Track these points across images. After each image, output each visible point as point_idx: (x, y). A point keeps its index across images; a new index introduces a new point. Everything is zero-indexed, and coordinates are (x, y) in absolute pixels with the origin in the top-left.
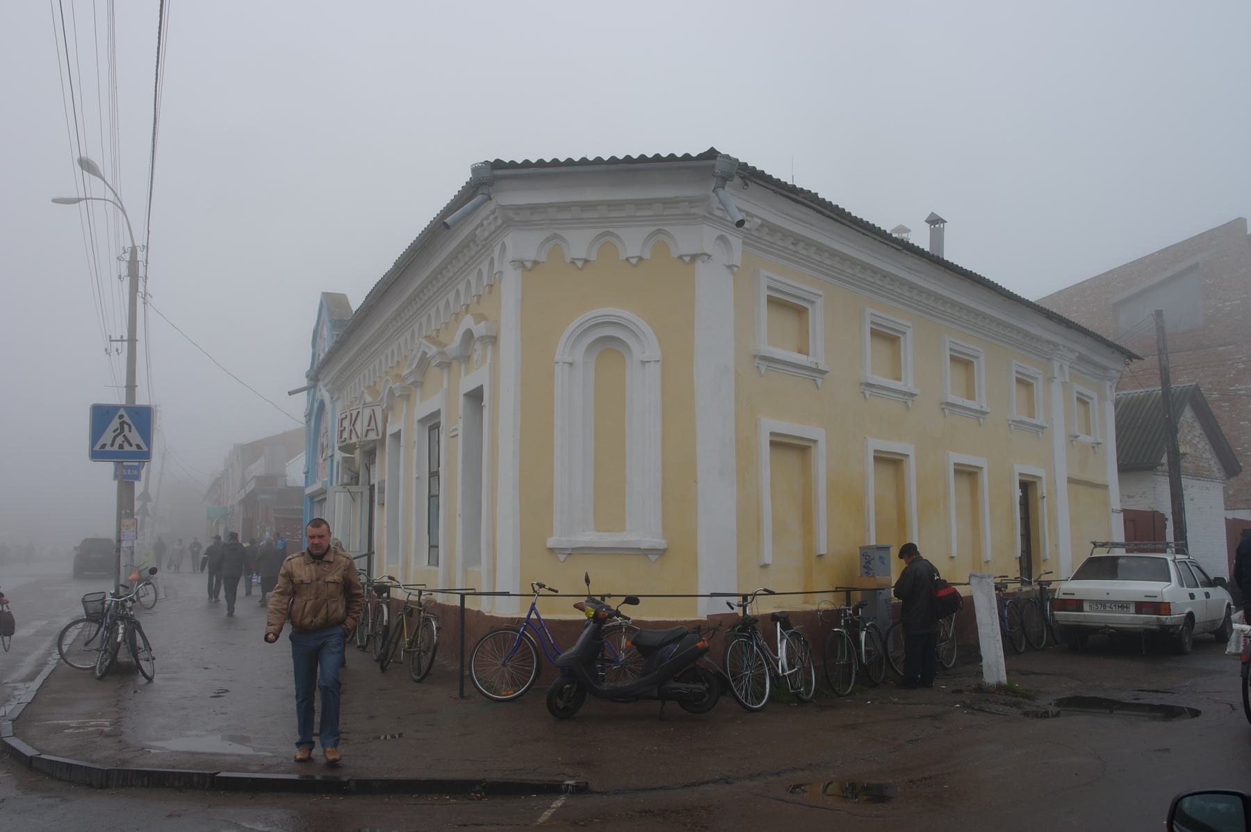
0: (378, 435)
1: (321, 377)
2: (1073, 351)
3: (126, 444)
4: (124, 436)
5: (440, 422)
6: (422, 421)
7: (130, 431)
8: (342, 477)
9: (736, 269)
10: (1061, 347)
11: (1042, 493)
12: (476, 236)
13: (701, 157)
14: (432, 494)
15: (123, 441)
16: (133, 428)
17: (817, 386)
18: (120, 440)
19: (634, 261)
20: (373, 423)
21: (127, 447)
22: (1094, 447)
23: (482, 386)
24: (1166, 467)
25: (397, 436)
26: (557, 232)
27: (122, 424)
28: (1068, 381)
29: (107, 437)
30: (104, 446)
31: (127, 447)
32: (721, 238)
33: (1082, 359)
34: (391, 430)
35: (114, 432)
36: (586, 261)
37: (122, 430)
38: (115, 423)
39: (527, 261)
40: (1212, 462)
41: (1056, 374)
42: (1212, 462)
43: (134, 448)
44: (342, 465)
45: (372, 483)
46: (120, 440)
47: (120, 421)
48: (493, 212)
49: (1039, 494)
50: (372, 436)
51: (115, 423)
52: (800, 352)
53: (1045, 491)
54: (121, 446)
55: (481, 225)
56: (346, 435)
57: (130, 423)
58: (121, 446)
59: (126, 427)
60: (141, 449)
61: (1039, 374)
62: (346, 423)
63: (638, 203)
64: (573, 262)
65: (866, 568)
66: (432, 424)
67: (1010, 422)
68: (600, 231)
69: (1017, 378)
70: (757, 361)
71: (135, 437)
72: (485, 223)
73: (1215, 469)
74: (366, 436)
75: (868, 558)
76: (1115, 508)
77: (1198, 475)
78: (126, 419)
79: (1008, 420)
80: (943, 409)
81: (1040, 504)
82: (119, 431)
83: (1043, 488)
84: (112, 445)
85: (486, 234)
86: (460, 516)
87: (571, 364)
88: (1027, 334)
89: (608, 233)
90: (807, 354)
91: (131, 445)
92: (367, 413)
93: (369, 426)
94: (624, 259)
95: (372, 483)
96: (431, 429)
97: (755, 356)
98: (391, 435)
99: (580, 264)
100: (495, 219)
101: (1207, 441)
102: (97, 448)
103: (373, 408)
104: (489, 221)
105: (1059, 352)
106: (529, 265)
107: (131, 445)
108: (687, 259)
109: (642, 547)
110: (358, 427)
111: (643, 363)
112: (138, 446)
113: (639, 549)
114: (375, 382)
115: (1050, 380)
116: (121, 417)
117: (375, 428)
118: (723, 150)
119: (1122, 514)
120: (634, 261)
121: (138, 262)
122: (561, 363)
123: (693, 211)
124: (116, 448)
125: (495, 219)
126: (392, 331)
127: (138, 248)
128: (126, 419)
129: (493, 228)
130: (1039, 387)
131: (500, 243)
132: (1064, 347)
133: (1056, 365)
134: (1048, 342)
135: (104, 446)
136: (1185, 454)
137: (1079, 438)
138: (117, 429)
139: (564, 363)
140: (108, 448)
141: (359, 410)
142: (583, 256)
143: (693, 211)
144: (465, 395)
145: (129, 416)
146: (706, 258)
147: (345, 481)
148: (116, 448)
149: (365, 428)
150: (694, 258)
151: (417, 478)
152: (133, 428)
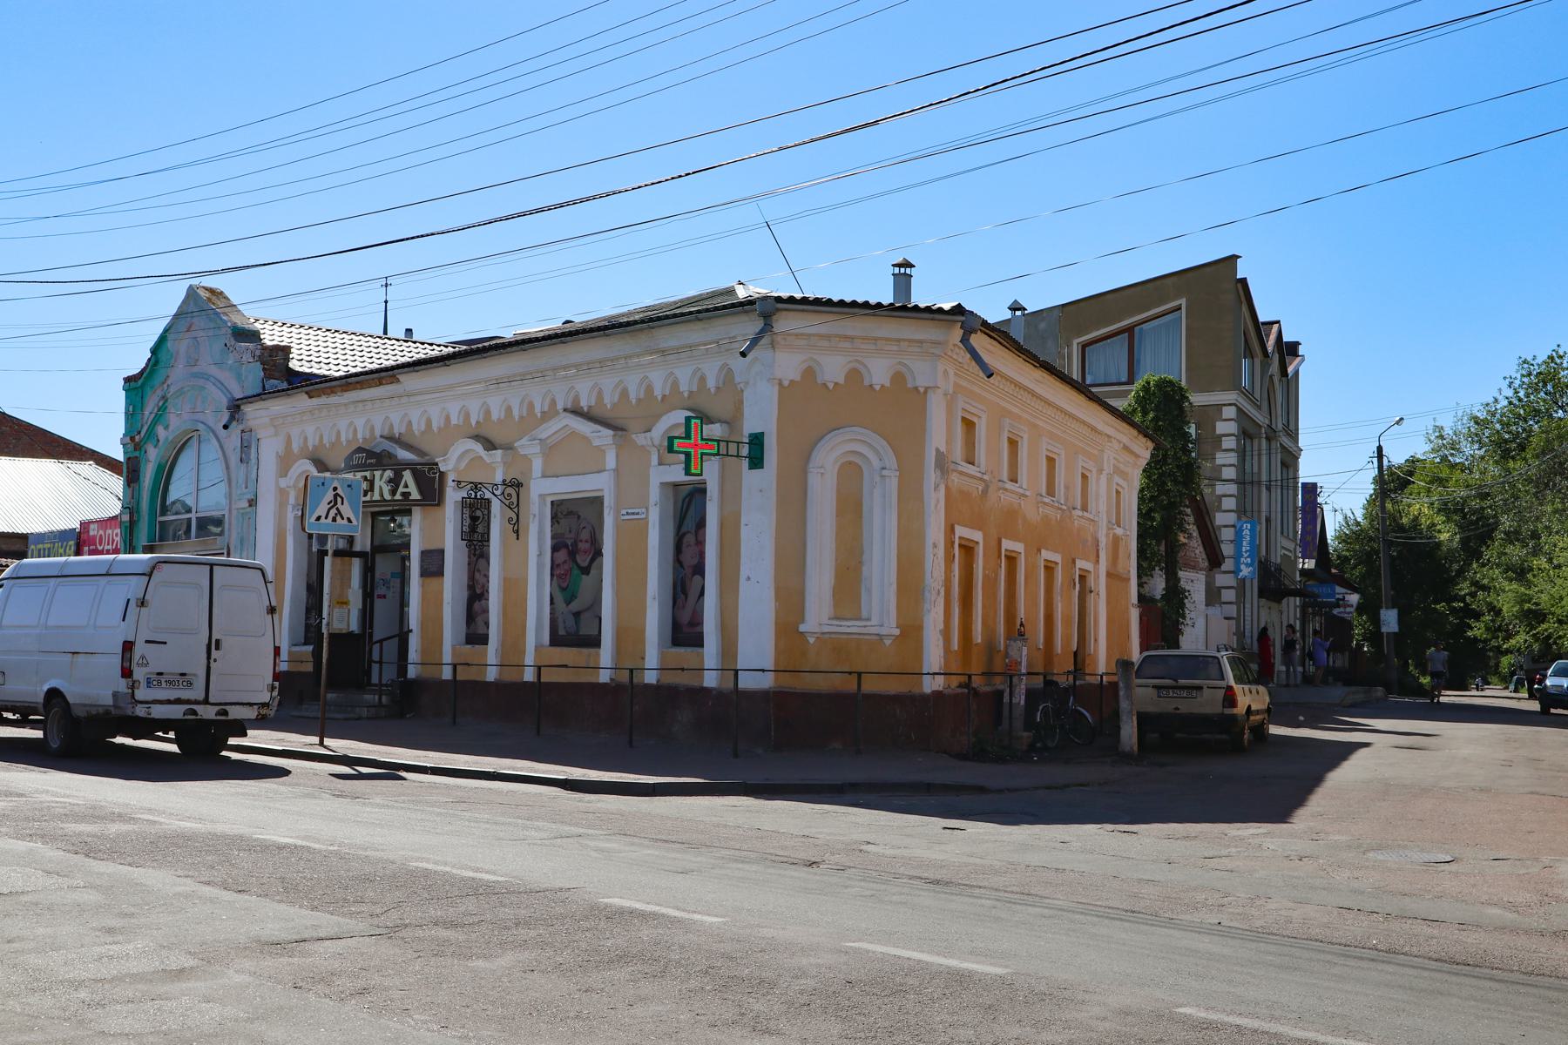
3: (338, 518)
4: (337, 509)
7: (342, 504)
18: (333, 512)
21: (338, 518)
27: (336, 496)
30: (318, 518)
33: (1126, 448)
35: (329, 504)
37: (336, 503)
40: (1197, 552)
41: (1105, 467)
46: (333, 512)
51: (330, 495)
54: (334, 520)
57: (342, 494)
58: (334, 520)
59: (339, 500)
78: (339, 491)
84: (326, 518)
88: (1093, 429)
90: (973, 464)
91: (343, 519)
94: (868, 384)
105: (1109, 444)
107: (343, 519)
108: (922, 390)
112: (349, 520)
116: (335, 489)
134: (1109, 436)
135: (318, 518)
138: (331, 502)
150: (927, 389)
152: (345, 499)
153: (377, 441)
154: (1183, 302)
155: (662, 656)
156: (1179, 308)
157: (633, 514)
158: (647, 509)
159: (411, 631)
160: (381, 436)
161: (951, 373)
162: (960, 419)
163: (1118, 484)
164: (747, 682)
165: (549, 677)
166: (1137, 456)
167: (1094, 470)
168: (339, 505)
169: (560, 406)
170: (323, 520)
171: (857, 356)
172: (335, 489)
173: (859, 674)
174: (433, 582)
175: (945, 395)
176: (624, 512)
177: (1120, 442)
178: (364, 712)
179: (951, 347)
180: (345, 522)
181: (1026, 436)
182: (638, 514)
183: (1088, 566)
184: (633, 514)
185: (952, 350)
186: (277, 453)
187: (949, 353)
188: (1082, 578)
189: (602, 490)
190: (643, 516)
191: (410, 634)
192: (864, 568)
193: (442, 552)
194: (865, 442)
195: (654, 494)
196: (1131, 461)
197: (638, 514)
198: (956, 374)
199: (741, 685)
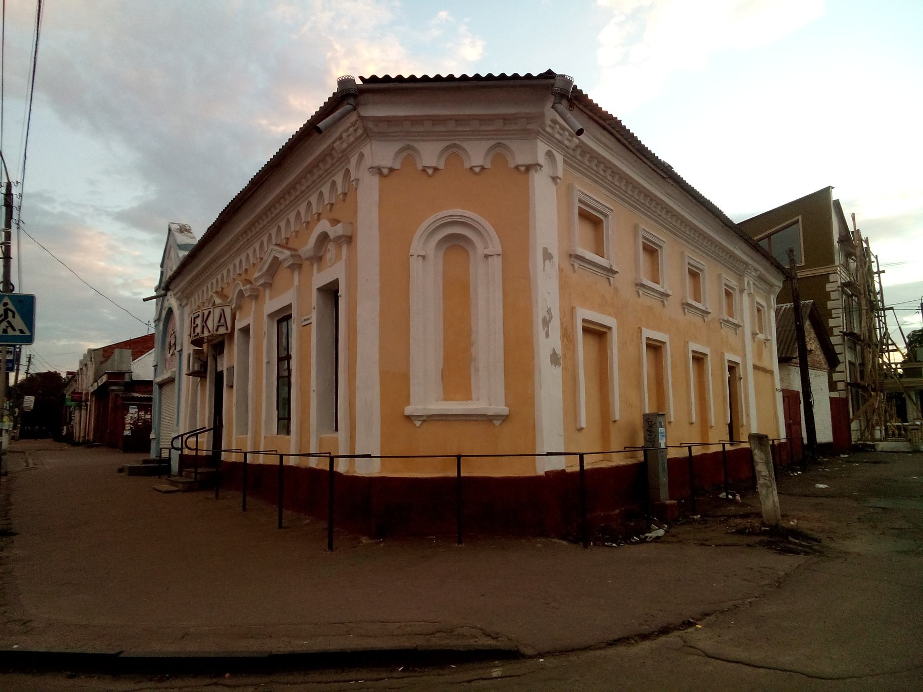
0: (227, 329)
1: (171, 287)
2: (756, 270)
3: (10, 330)
4: (9, 322)
5: (291, 314)
6: (271, 316)
7: (14, 317)
8: (193, 366)
9: (558, 181)
11: (740, 375)
12: (334, 149)
13: (541, 76)
14: (280, 376)
15: (7, 327)
16: (17, 315)
17: (610, 283)
19: (477, 170)
20: (222, 321)
21: (10, 330)
22: (765, 343)
23: (337, 280)
24: (797, 361)
25: (246, 331)
26: (411, 143)
31: (10, 332)
32: (549, 154)
33: (761, 278)
34: (239, 325)
37: (6, 316)
39: (384, 168)
41: (746, 287)
42: (821, 357)
43: (18, 333)
44: (193, 355)
45: (219, 369)
47: (5, 308)
48: (353, 125)
49: (737, 375)
50: (222, 331)
55: (340, 138)
56: (198, 330)
57: (13, 309)
59: (10, 314)
60: (25, 333)
61: (737, 286)
62: (199, 321)
63: (482, 119)
64: (424, 170)
65: (649, 431)
66: (283, 318)
67: (721, 321)
68: (448, 143)
70: (573, 259)
71: (18, 322)
72: (345, 135)
73: (823, 362)
74: (217, 331)
75: (650, 423)
77: (815, 367)
78: (10, 306)
81: (738, 384)
82: (3, 317)
83: (740, 371)
85: (345, 145)
86: (314, 391)
87: (424, 257)
89: (454, 145)
91: (14, 330)
92: (217, 312)
94: (469, 167)
95: (219, 369)
96: (279, 322)
97: (570, 256)
98: (239, 330)
99: (430, 171)
100: (355, 131)
101: (818, 342)
103: (223, 308)
104: (348, 134)
106: (385, 171)
107: (14, 330)
108: (523, 169)
110: (210, 323)
112: (21, 331)
113: (485, 416)
114: (222, 289)
115: (742, 291)
117: (225, 324)
118: (557, 71)
119: (781, 392)
120: (477, 170)
121: (12, 194)
122: (415, 256)
123: (530, 127)
125: (355, 131)
126: (242, 243)
127: (12, 184)
128: (10, 306)
129: (352, 139)
130: (736, 296)
131: (358, 153)
132: (752, 266)
136: (811, 351)
139: (418, 256)
141: (210, 310)
142: (434, 165)
143: (530, 127)
144: (319, 289)
145: (13, 304)
146: (539, 168)
147: (196, 369)
149: (216, 324)
150: (528, 168)
151: (268, 363)
152: (17, 315)
154: (800, 218)
156: (797, 222)
161: (559, 158)
163: (758, 303)
166: (771, 285)
167: (737, 289)
168: (10, 318)
171: (455, 140)
173: (459, 457)
175: (554, 179)
177: (756, 270)
181: (665, 246)
188: (732, 368)
192: (473, 350)
196: (767, 288)
198: (565, 161)
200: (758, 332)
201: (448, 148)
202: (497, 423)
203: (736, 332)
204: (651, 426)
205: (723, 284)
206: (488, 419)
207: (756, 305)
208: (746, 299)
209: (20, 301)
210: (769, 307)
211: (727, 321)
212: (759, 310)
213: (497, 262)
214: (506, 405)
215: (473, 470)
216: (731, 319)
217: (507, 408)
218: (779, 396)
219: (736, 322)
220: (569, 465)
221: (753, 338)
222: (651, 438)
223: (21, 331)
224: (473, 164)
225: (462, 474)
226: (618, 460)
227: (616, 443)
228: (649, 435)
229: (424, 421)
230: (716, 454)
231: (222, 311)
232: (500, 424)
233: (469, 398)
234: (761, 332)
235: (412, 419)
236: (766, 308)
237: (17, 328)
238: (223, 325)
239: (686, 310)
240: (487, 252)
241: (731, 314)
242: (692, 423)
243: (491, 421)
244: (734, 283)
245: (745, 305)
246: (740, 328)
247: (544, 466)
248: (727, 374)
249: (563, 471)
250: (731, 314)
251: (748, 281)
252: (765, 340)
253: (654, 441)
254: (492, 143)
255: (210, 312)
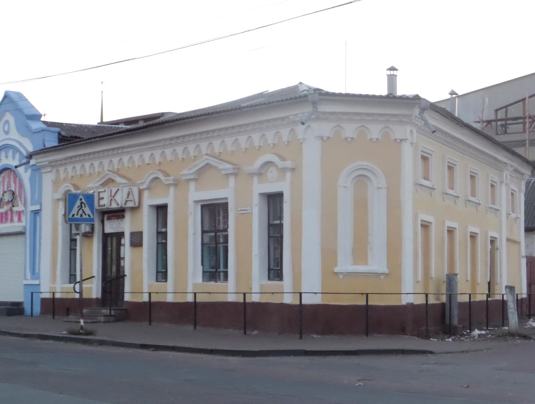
0: (135, 204)
2: (512, 166)
3: (83, 215)
4: (83, 210)
7: (85, 207)
10: (508, 165)
16: (86, 206)
18: (81, 212)
19: (375, 140)
20: (131, 197)
21: (84, 216)
27: (82, 203)
28: (508, 183)
29: (75, 210)
30: (73, 215)
31: (84, 216)
33: (516, 171)
35: (78, 207)
36: (352, 139)
38: (78, 203)
39: (325, 137)
41: (504, 180)
43: (87, 217)
49: (496, 247)
51: (78, 203)
52: (425, 179)
53: (498, 245)
54: (81, 216)
58: (81, 216)
59: (83, 205)
61: (498, 180)
64: (346, 139)
65: (449, 284)
67: (487, 208)
69: (470, 175)
70: (417, 186)
71: (87, 210)
72: (300, 115)
74: (125, 204)
76: (523, 255)
78: (83, 201)
79: (486, 207)
80: (466, 203)
82: (80, 207)
84: (77, 215)
88: (496, 159)
90: (428, 180)
91: (85, 214)
92: (126, 190)
93: (128, 198)
99: (349, 140)
102: (70, 216)
105: (507, 167)
106: (325, 139)
107: (85, 214)
108: (399, 141)
109: (379, 272)
111: (379, 188)
112: (89, 215)
113: (377, 273)
114: (118, 169)
115: (501, 182)
116: (81, 199)
118: (422, 96)
120: (375, 140)
124: (79, 216)
126: (162, 144)
128: (83, 201)
130: (497, 186)
132: (509, 164)
133: (505, 174)
135: (73, 215)
137: (511, 215)
140: (75, 216)
145: (85, 199)
148: (79, 216)
150: (401, 140)
152: (86, 206)
153: (106, 173)
155: (262, 286)
157: (244, 210)
158: (252, 207)
159: (126, 275)
160: (108, 171)
161: (415, 131)
162: (420, 156)
163: (512, 189)
164: (307, 300)
165: (201, 299)
166: (523, 174)
167: (498, 182)
168: (83, 208)
169: (204, 152)
170: (75, 216)
172: (81, 199)
173: (367, 294)
174: (137, 249)
175: (412, 144)
176: (239, 209)
177: (512, 166)
178: (102, 319)
179: (414, 117)
180: (87, 217)
182: (247, 210)
183: (496, 235)
184: (244, 210)
185: (414, 119)
186: (52, 180)
187: (413, 121)
188: (493, 242)
189: (227, 198)
190: (249, 212)
191: (125, 277)
193: (141, 233)
194: (367, 169)
195: (256, 200)
197: (247, 210)
198: (417, 132)
199: (304, 302)
200: (511, 213)
201: (359, 127)
202: (382, 277)
203: (496, 214)
204: (450, 281)
205: (490, 180)
206: (378, 275)
207: (510, 191)
208: (504, 188)
209: (88, 197)
210: (520, 191)
211: (492, 208)
212: (512, 194)
213: (384, 192)
214: (387, 268)
215: (374, 301)
216: (493, 206)
217: (388, 270)
218: (524, 262)
219: (497, 208)
220: (420, 300)
221: (507, 217)
222: (450, 288)
223: (89, 215)
224: (373, 137)
225: (369, 303)
226: (432, 300)
227: (431, 290)
228: (449, 286)
229: (344, 275)
230: (480, 302)
231: (130, 190)
232: (384, 278)
233: (366, 263)
234: (513, 212)
235: (338, 274)
236: (517, 192)
237: (87, 213)
238: (132, 201)
239: (467, 204)
240: (380, 186)
241: (493, 203)
242: (467, 281)
243: (379, 276)
244: (496, 179)
245: (503, 192)
246: (499, 211)
247: (406, 300)
248: (489, 247)
249: (412, 303)
250: (493, 203)
251: (506, 175)
252: (515, 218)
253: (452, 290)
254: (384, 126)
255: (118, 189)
